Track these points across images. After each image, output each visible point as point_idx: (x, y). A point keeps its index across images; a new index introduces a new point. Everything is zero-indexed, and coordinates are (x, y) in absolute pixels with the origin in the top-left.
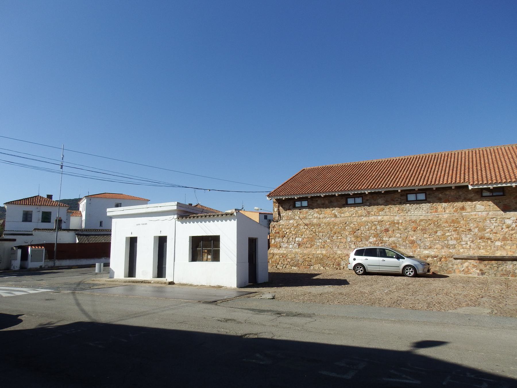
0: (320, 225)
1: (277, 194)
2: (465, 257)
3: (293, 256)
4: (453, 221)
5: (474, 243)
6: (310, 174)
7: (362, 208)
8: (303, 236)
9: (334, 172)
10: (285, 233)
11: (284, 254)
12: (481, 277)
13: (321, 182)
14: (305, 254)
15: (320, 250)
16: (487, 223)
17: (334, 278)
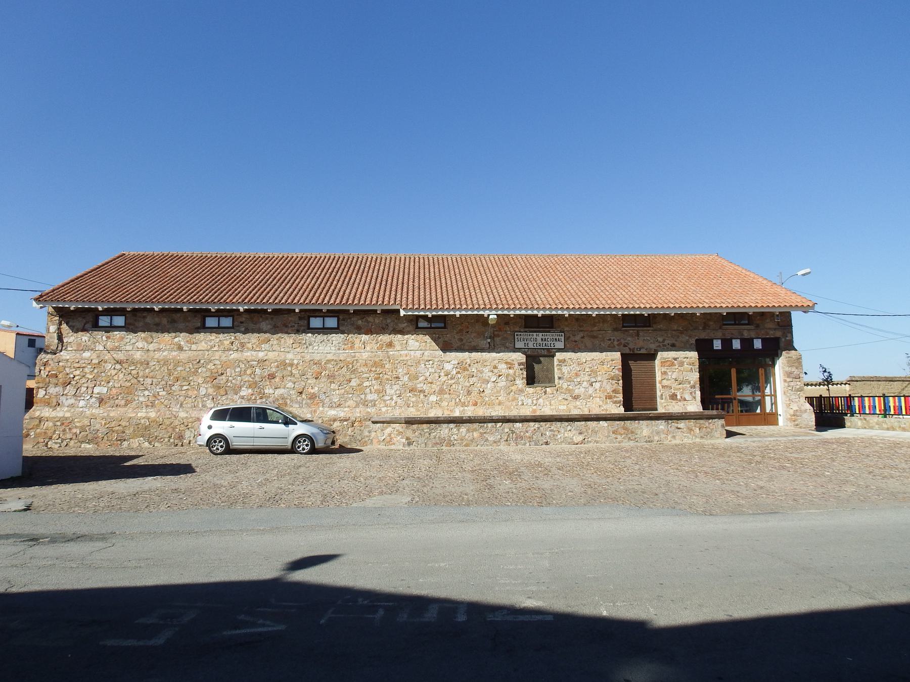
0: (148, 364)
1: (58, 298)
2: (388, 420)
3: (86, 422)
4: (375, 364)
5: (401, 397)
6: (135, 264)
7: (231, 335)
8: (111, 383)
9: (184, 267)
10: (72, 376)
11: (67, 418)
13: (155, 283)
14: (113, 419)
15: (144, 410)
16: (421, 368)
17: (167, 463)
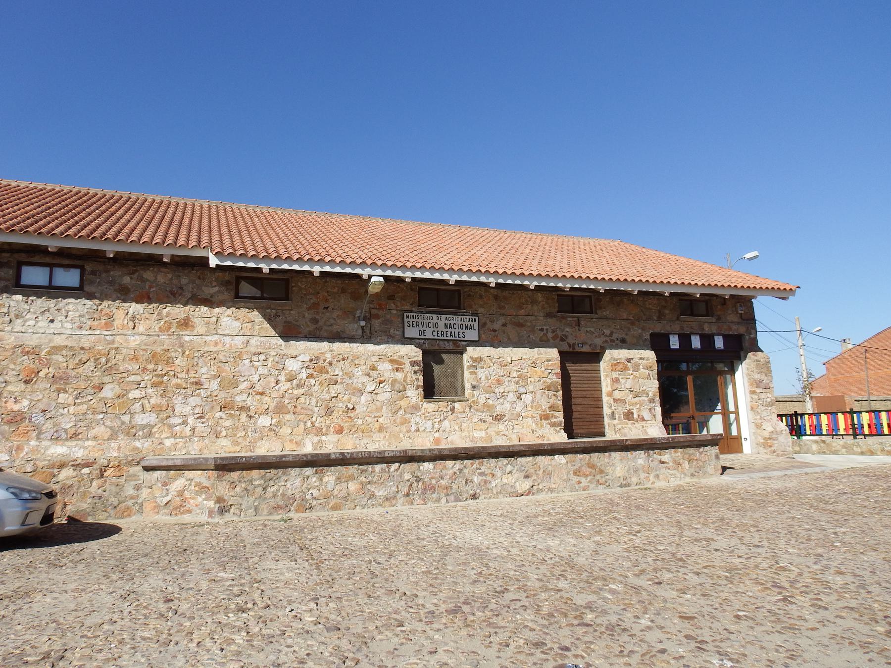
2: (178, 463)
4: (154, 357)
5: (204, 420)
12: (216, 520)
16: (244, 368)
